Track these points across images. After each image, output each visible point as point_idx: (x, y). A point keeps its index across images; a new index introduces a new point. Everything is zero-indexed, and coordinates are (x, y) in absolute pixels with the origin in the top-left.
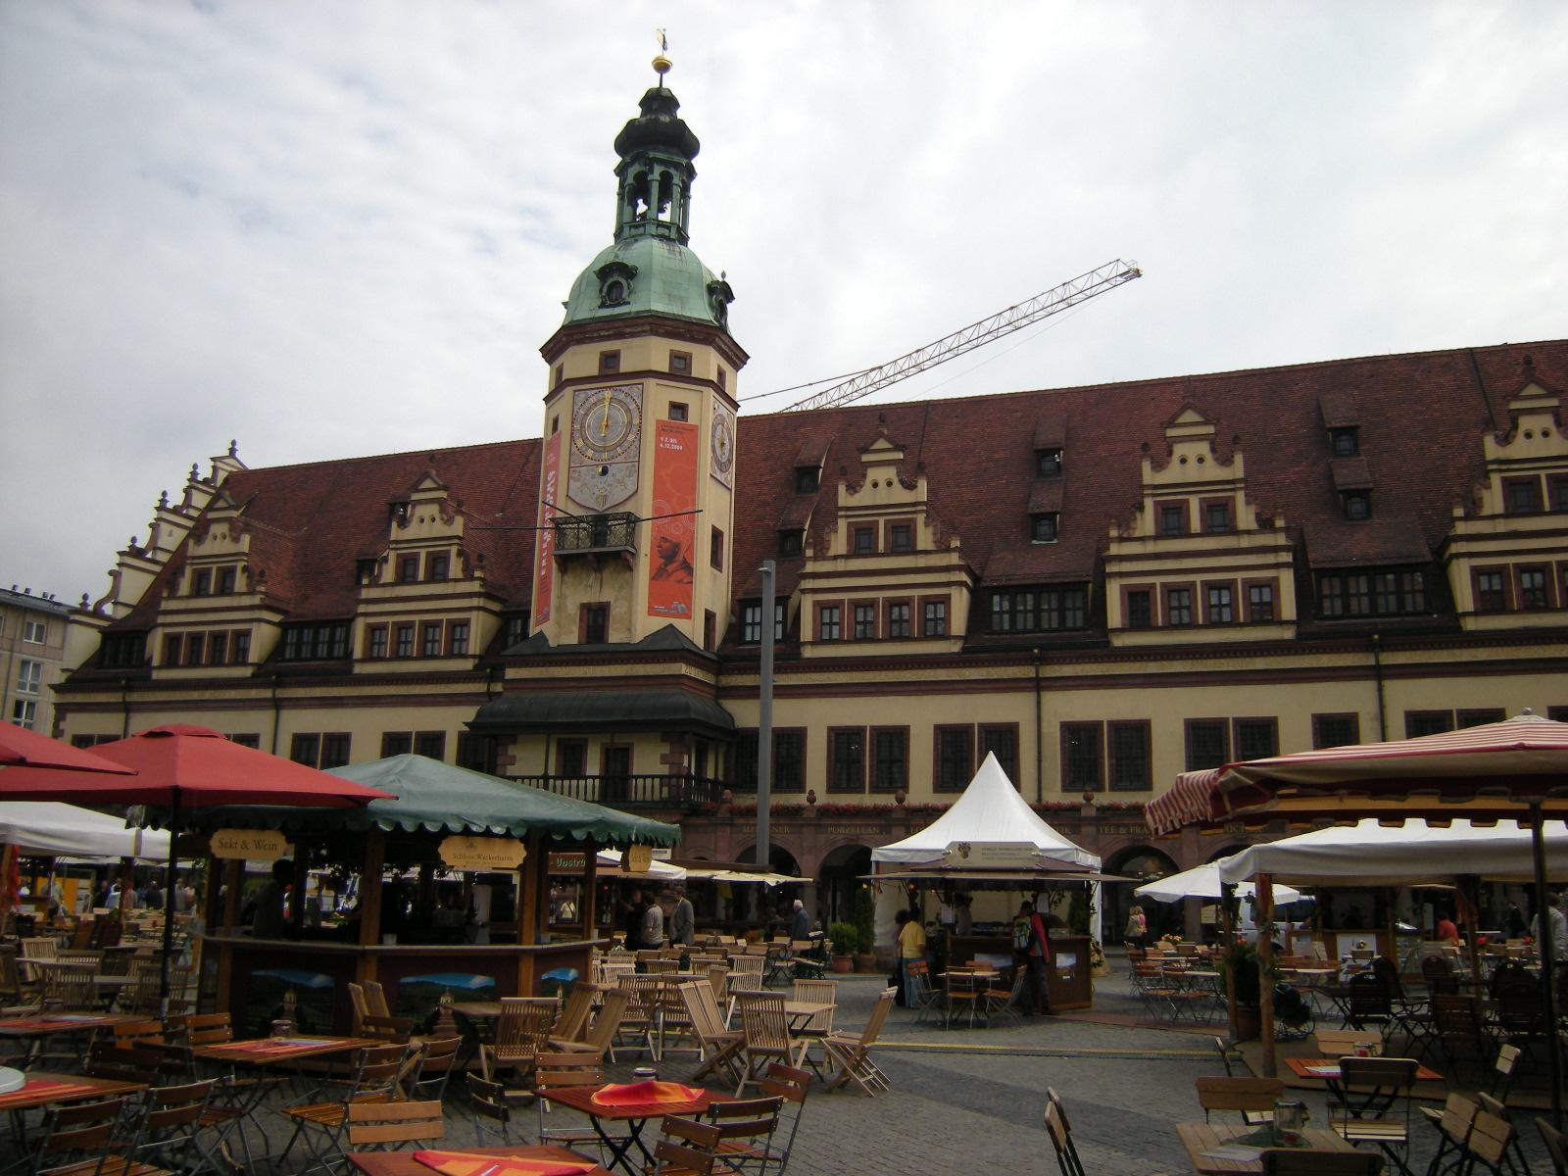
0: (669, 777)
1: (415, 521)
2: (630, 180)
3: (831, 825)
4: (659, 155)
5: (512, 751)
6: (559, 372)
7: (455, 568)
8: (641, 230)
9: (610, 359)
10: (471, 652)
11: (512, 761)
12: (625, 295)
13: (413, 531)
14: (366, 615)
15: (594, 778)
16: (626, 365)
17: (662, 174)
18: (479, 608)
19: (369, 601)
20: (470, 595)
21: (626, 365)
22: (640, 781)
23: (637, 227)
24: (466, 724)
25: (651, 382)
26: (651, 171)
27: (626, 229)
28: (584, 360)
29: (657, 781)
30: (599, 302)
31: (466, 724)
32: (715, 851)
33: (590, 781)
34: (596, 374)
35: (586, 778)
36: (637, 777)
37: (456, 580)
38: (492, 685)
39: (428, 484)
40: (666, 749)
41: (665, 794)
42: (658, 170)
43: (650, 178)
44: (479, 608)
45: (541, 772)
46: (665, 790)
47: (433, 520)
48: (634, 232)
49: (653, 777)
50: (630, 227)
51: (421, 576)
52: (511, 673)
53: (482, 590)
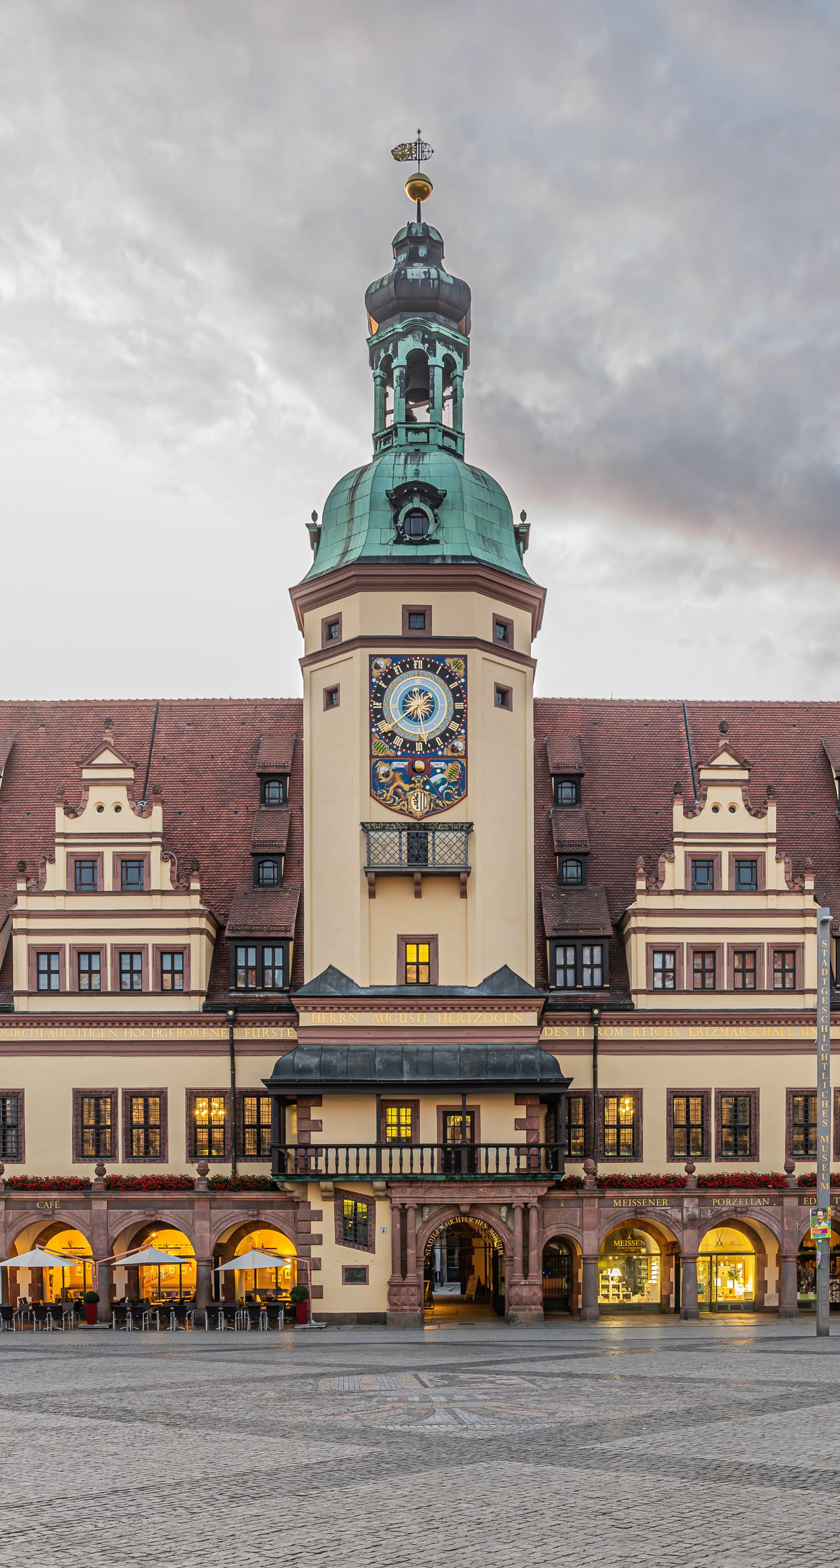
0: (528, 1146)
1: (91, 807)
2: (400, 360)
3: (718, 1197)
4: (446, 332)
5: (316, 1113)
6: (332, 625)
7: (160, 874)
8: (422, 437)
9: (417, 617)
10: (194, 987)
11: (318, 1126)
12: (431, 529)
13: (89, 821)
14: (28, 932)
15: (432, 1146)
16: (438, 629)
17: (447, 358)
18: (201, 931)
19: (28, 914)
20: (188, 913)
21: (438, 629)
22: (492, 1151)
23: (417, 431)
24: (263, 1081)
25: (475, 655)
26: (433, 351)
27: (402, 432)
28: (374, 613)
29: (512, 1150)
30: (393, 534)
31: (263, 1081)
32: (582, 1227)
33: (427, 1152)
34: (399, 633)
35: (422, 1147)
36: (487, 1146)
37: (163, 893)
38: (235, 1030)
39: (107, 757)
40: (521, 1112)
41: (523, 1165)
42: (441, 350)
43: (431, 361)
44: (201, 931)
45: (373, 1140)
46: (523, 1159)
47: (118, 809)
48: (412, 437)
49: (508, 1146)
50: (408, 430)
51: (108, 884)
52: (307, 1019)
53: (201, 907)
